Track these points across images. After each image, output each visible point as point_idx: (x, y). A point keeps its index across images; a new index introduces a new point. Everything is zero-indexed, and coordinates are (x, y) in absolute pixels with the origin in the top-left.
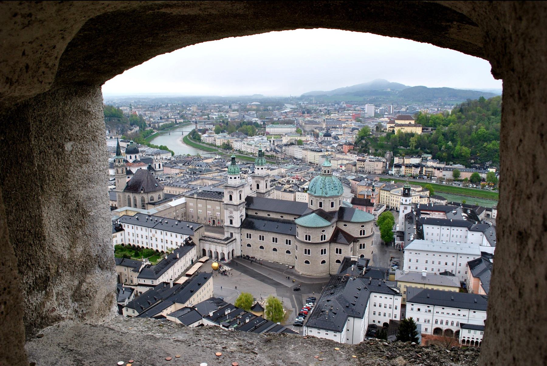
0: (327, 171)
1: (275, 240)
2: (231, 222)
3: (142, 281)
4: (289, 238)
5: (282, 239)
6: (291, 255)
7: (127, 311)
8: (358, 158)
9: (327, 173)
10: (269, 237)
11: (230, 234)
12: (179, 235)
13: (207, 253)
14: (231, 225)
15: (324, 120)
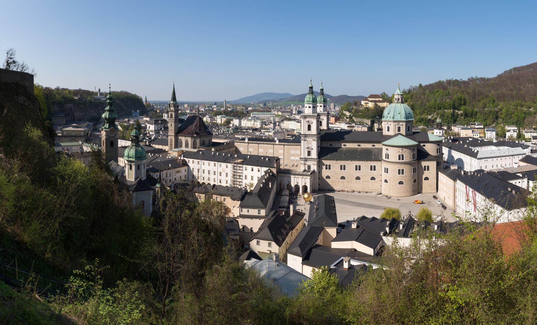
0: (400, 99)
1: (358, 168)
2: (309, 153)
3: (245, 212)
4: (373, 163)
5: (365, 165)
6: (377, 182)
7: (258, 243)
8: (347, 125)
9: (400, 101)
10: (351, 165)
11: (307, 166)
12: (256, 168)
13: (286, 187)
14: (309, 157)
15: (296, 109)
